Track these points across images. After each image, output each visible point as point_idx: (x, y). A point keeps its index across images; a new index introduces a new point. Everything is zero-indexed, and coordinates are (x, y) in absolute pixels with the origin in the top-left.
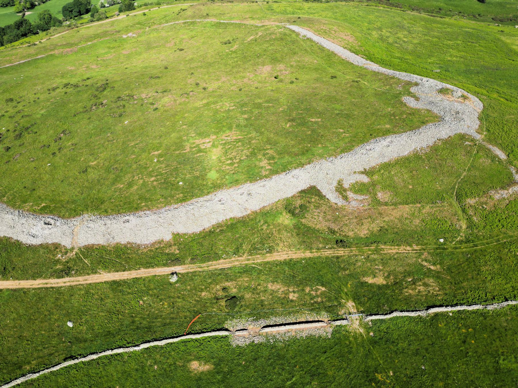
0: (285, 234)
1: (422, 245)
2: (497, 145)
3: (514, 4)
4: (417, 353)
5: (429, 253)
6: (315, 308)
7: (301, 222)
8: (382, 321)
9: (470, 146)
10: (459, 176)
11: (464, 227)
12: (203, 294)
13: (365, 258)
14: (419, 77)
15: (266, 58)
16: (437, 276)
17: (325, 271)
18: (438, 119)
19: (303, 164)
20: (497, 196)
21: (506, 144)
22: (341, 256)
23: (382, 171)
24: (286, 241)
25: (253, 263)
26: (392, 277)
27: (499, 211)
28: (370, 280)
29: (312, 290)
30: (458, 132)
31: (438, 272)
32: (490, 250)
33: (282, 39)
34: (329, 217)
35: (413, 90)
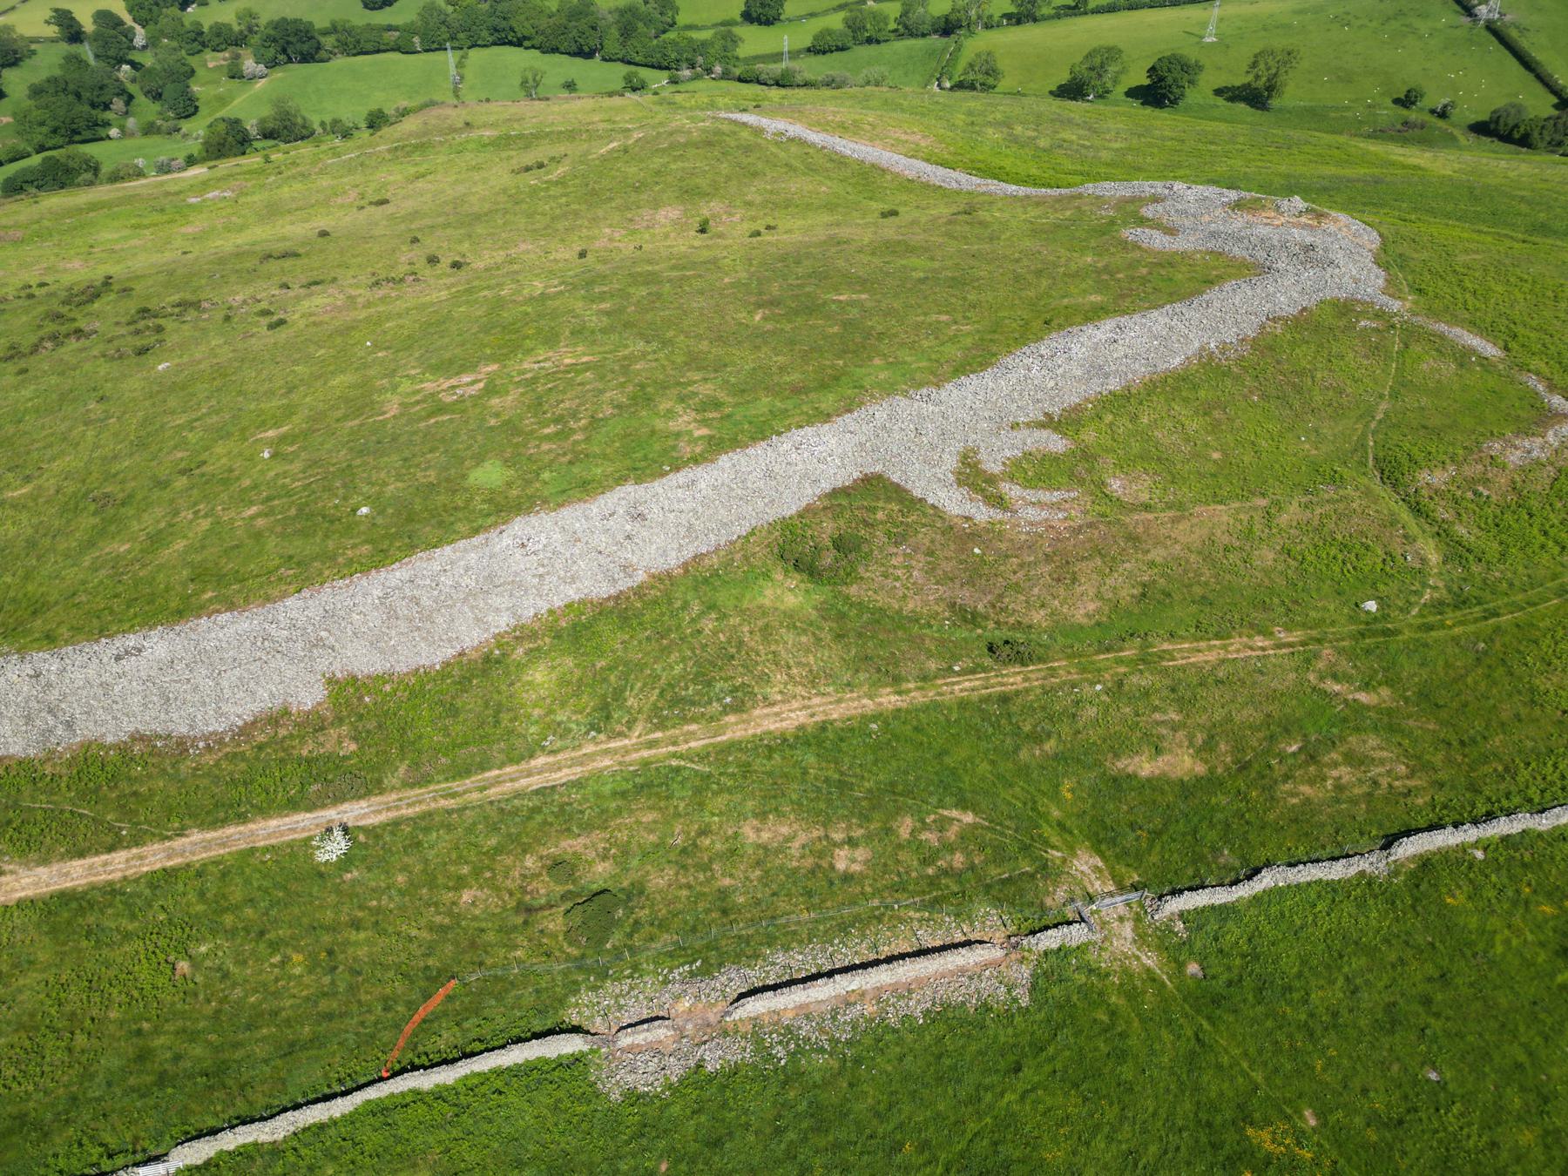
0: (790, 637)
1: (1304, 625)
2: (1455, 321)
3: (1348, 108)
4: (1391, 1020)
5: (1340, 651)
6: (945, 893)
7: (847, 597)
8: (1223, 912)
9: (1377, 330)
10: (1370, 413)
11: (1434, 558)
12: (466, 896)
13: (1107, 692)
14: (1159, 184)
15: (663, 191)
16: (1388, 722)
17: (962, 753)
18: (1255, 269)
19: (829, 415)
20: (1514, 457)
21: (1489, 320)
22: (1017, 693)
23: (1109, 418)
24: (799, 664)
25: (674, 755)
26: (1223, 747)
27: (1535, 504)
28: (1145, 766)
29: (925, 826)
30: (1328, 295)
31: (1389, 712)
32: (1547, 623)
34: (947, 566)
35: (1148, 212)
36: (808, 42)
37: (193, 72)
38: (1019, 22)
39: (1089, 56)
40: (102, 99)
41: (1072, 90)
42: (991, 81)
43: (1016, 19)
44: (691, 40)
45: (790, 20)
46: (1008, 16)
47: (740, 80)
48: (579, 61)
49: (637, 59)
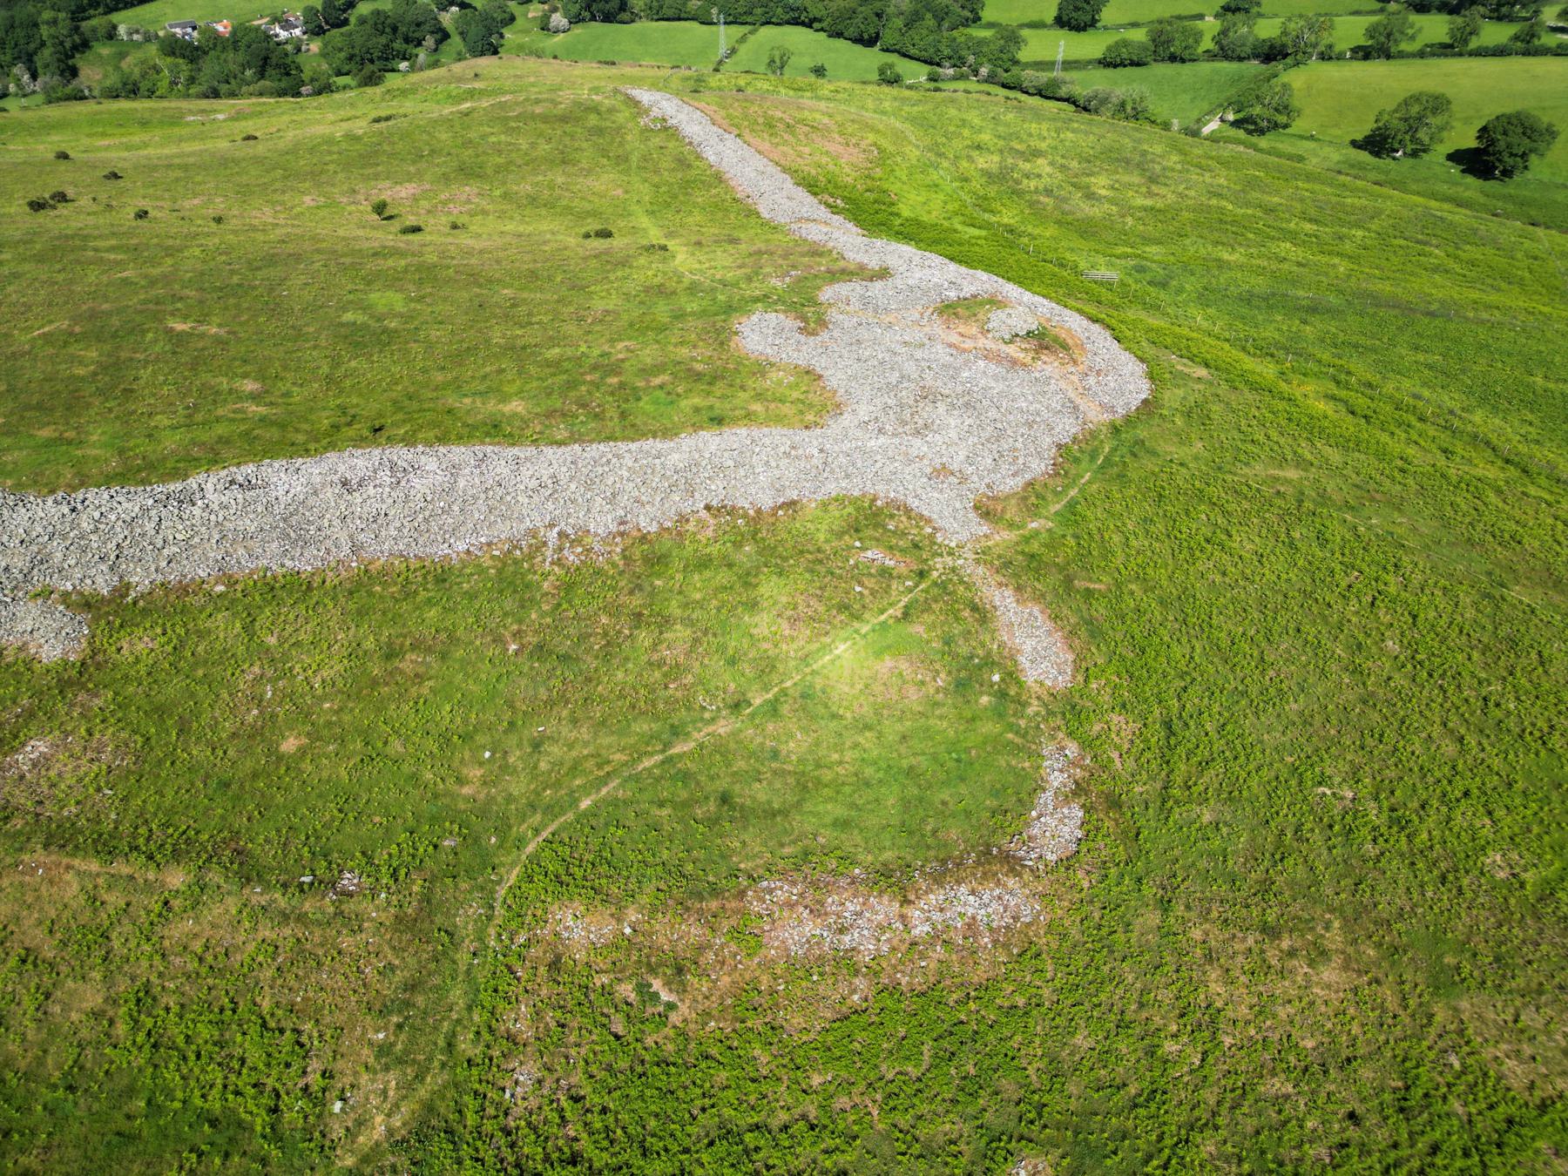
9: (885, 573)
20: (797, 933)
33: (564, 119)
36: (1099, 55)
37: (513, 19)
38: (1367, 57)
39: (1406, 103)
40: (417, 35)
41: (1377, 144)
42: (1282, 119)
43: (1364, 53)
44: (970, 38)
45: (1106, 28)
46: (1355, 50)
47: (1004, 86)
48: (858, 48)
49: (913, 51)
